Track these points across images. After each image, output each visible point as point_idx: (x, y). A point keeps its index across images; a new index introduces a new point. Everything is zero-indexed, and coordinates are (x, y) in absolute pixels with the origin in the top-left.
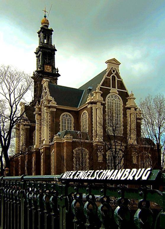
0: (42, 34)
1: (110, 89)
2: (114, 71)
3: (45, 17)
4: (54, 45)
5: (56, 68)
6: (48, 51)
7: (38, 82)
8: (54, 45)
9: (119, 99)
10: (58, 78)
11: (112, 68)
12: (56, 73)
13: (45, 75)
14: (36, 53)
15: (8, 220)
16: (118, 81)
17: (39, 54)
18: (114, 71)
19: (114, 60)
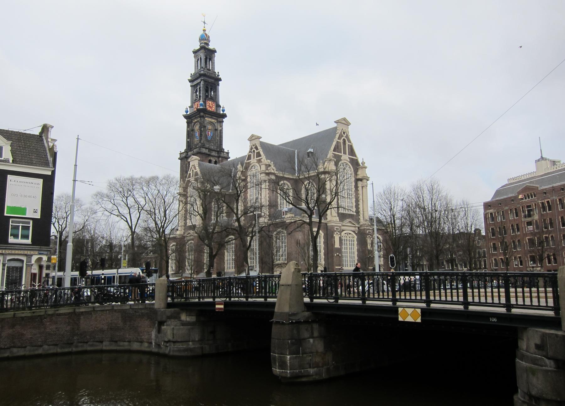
1: (341, 156)
2: (344, 133)
3: (204, 31)
4: (218, 73)
5: (222, 106)
6: (210, 80)
7: (193, 124)
8: (218, 73)
9: (350, 167)
11: (342, 129)
13: (207, 115)
14: (190, 81)
15: (347, 313)
16: (348, 145)
17: (195, 83)
18: (344, 133)
19: (345, 119)
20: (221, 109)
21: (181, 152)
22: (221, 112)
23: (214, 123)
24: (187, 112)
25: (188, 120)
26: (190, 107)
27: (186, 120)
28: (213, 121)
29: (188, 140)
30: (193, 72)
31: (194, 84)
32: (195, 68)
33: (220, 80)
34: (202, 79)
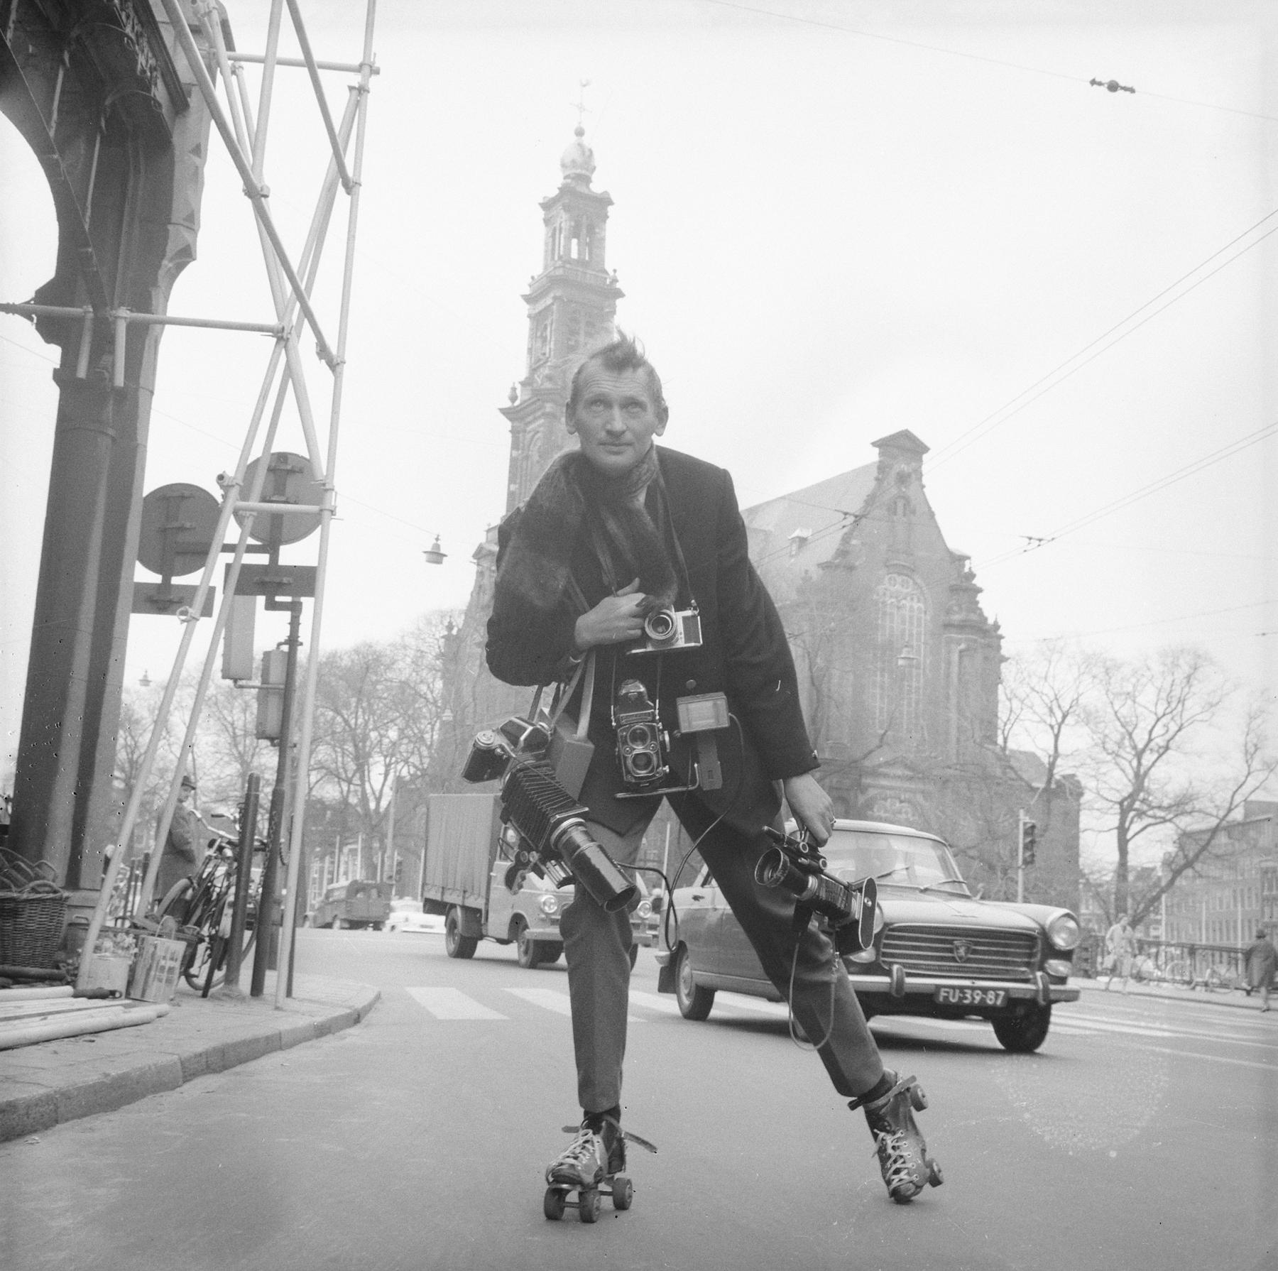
0: (564, 216)
3: (580, 133)
4: (615, 271)
8: (615, 271)
14: (528, 299)
17: (541, 306)
19: (906, 435)
21: (489, 525)
24: (513, 399)
25: (517, 424)
27: (508, 425)
29: (513, 487)
30: (538, 270)
31: (537, 311)
32: (546, 259)
33: (619, 294)
34: (559, 293)
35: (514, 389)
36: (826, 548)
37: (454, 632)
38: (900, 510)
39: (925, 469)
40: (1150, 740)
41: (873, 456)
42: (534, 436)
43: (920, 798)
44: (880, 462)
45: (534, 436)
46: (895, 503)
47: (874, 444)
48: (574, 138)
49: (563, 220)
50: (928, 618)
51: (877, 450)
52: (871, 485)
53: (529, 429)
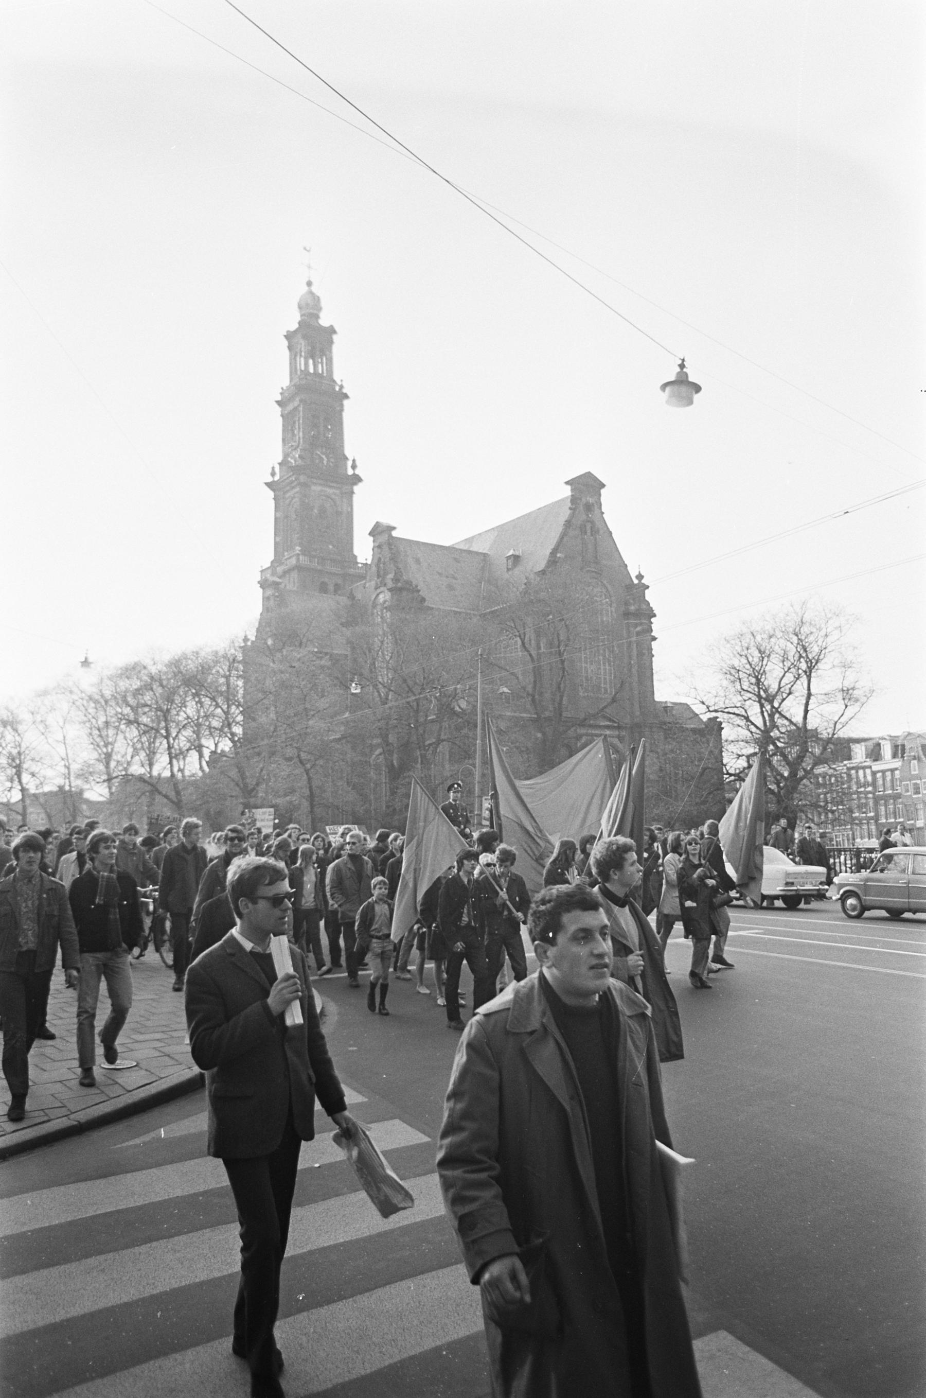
0: (303, 342)
3: (309, 284)
4: (342, 381)
5: (351, 458)
8: (342, 381)
10: (356, 488)
12: (350, 472)
13: (315, 481)
17: (290, 407)
19: (589, 475)
20: (350, 463)
22: (350, 472)
23: (333, 497)
24: (273, 474)
26: (280, 464)
27: (272, 494)
28: (330, 491)
30: (285, 382)
33: (346, 396)
35: (273, 468)
36: (539, 558)
37: (249, 643)
38: (589, 532)
39: (603, 499)
40: (780, 688)
41: (567, 492)
42: (291, 501)
43: (616, 741)
44: (572, 496)
45: (291, 501)
46: (585, 526)
47: (567, 483)
48: (306, 288)
49: (302, 345)
50: (613, 609)
51: (569, 488)
52: (565, 514)
53: (287, 495)
